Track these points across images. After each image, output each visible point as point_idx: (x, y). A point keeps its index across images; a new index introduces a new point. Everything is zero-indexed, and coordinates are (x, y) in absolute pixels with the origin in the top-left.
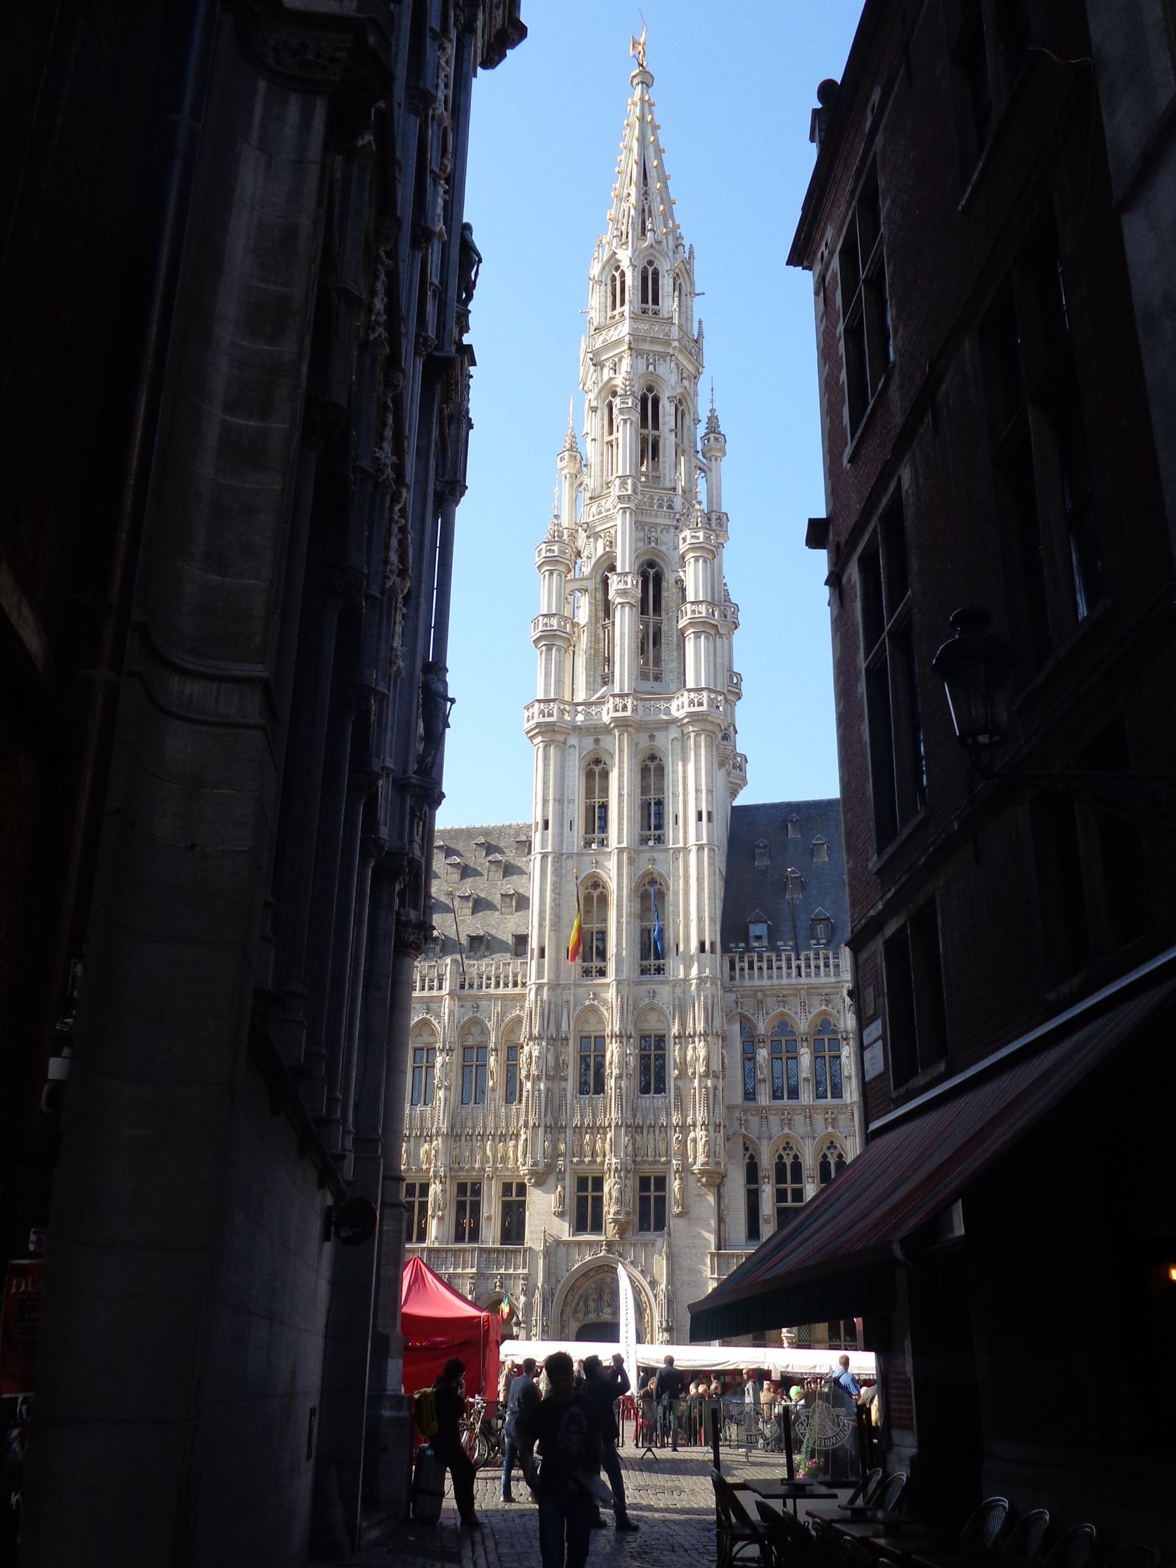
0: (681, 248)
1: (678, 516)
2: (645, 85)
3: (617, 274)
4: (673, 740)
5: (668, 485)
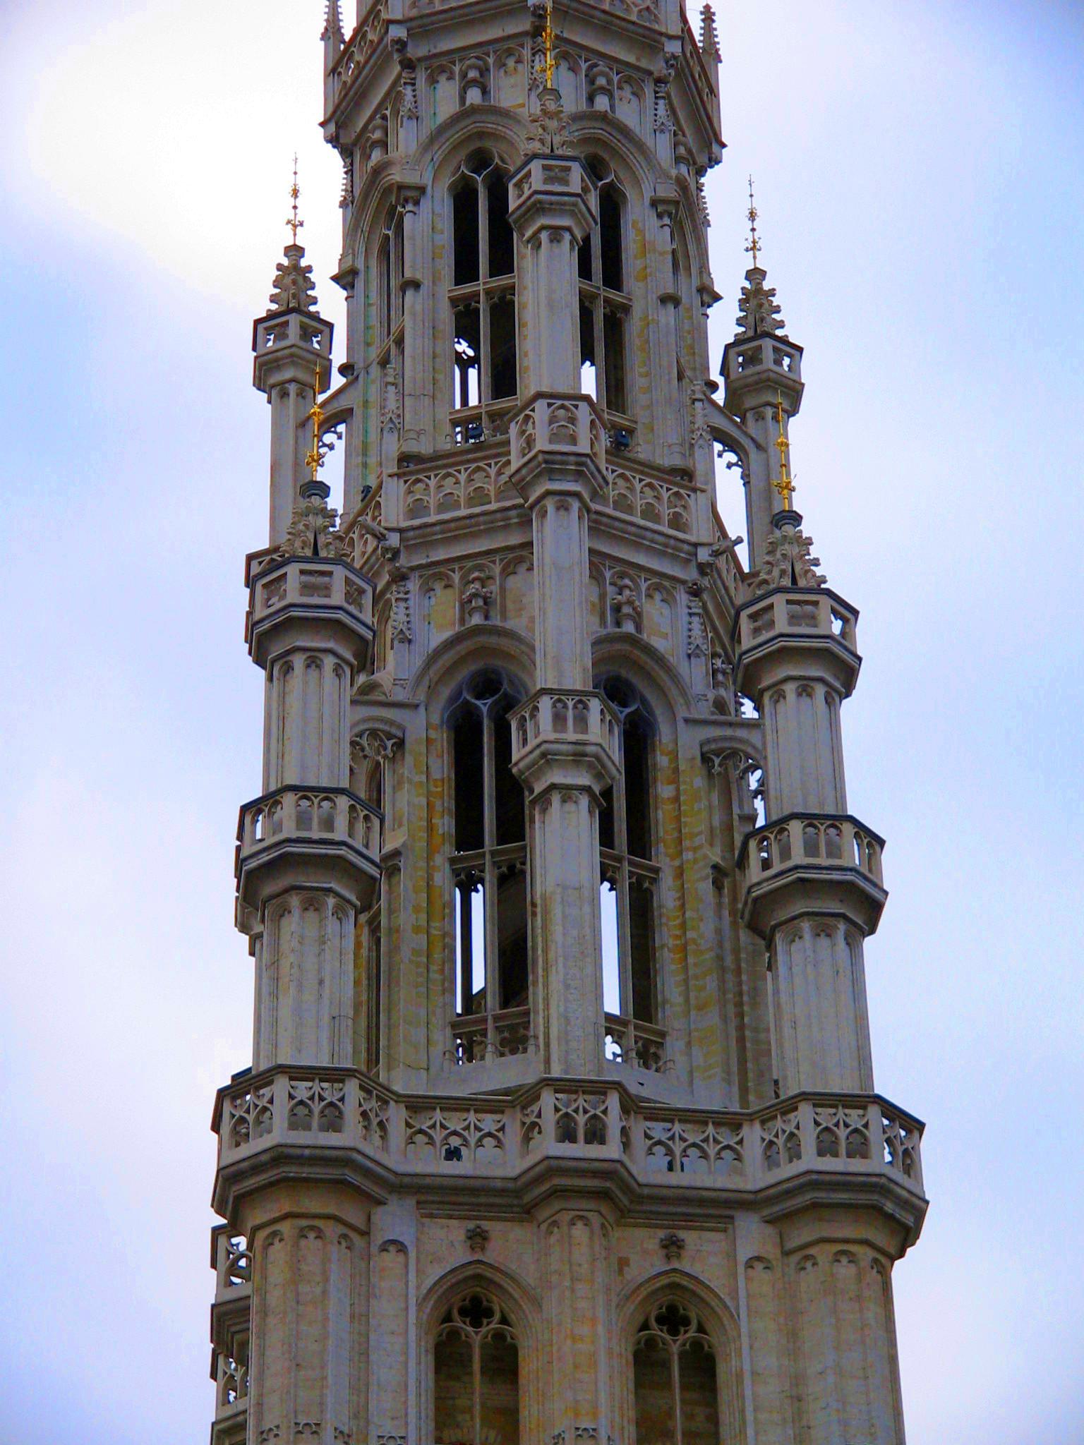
1: (703, 555)
4: (749, 1264)
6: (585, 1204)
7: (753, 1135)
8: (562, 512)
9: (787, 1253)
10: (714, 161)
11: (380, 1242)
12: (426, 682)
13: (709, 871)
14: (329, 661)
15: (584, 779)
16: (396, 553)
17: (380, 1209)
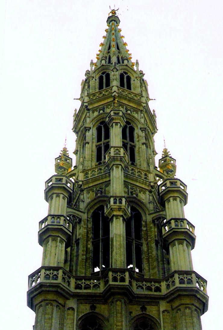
1: (152, 184)
3: (104, 76)
4: (163, 312)
6: (119, 297)
9: (173, 309)
10: (155, 132)
11: (67, 308)
12: (87, 209)
13: (154, 241)
14: (61, 196)
15: (121, 213)
16: (81, 185)
17: (68, 301)
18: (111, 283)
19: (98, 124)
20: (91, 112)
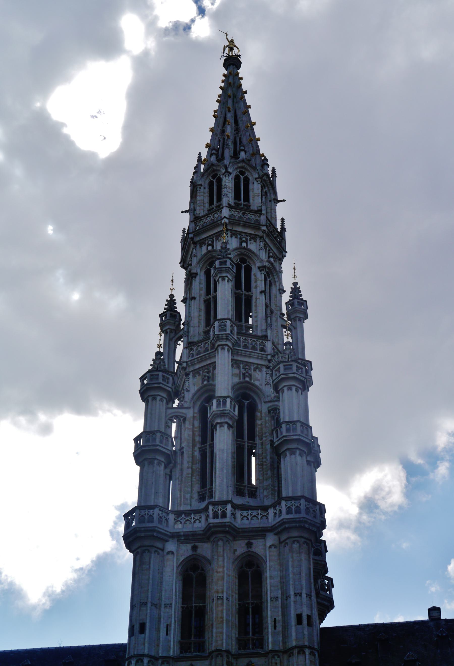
0: (266, 167)
1: (269, 357)
2: (235, 66)
3: (214, 181)
4: (270, 547)
5: (260, 334)
7: (271, 512)
8: (223, 350)
9: (280, 542)
11: (167, 552)
12: (193, 402)
13: (269, 442)
15: (227, 420)
16: (185, 368)
17: (167, 543)
18: (211, 520)
19: (206, 267)
20: (198, 247)
